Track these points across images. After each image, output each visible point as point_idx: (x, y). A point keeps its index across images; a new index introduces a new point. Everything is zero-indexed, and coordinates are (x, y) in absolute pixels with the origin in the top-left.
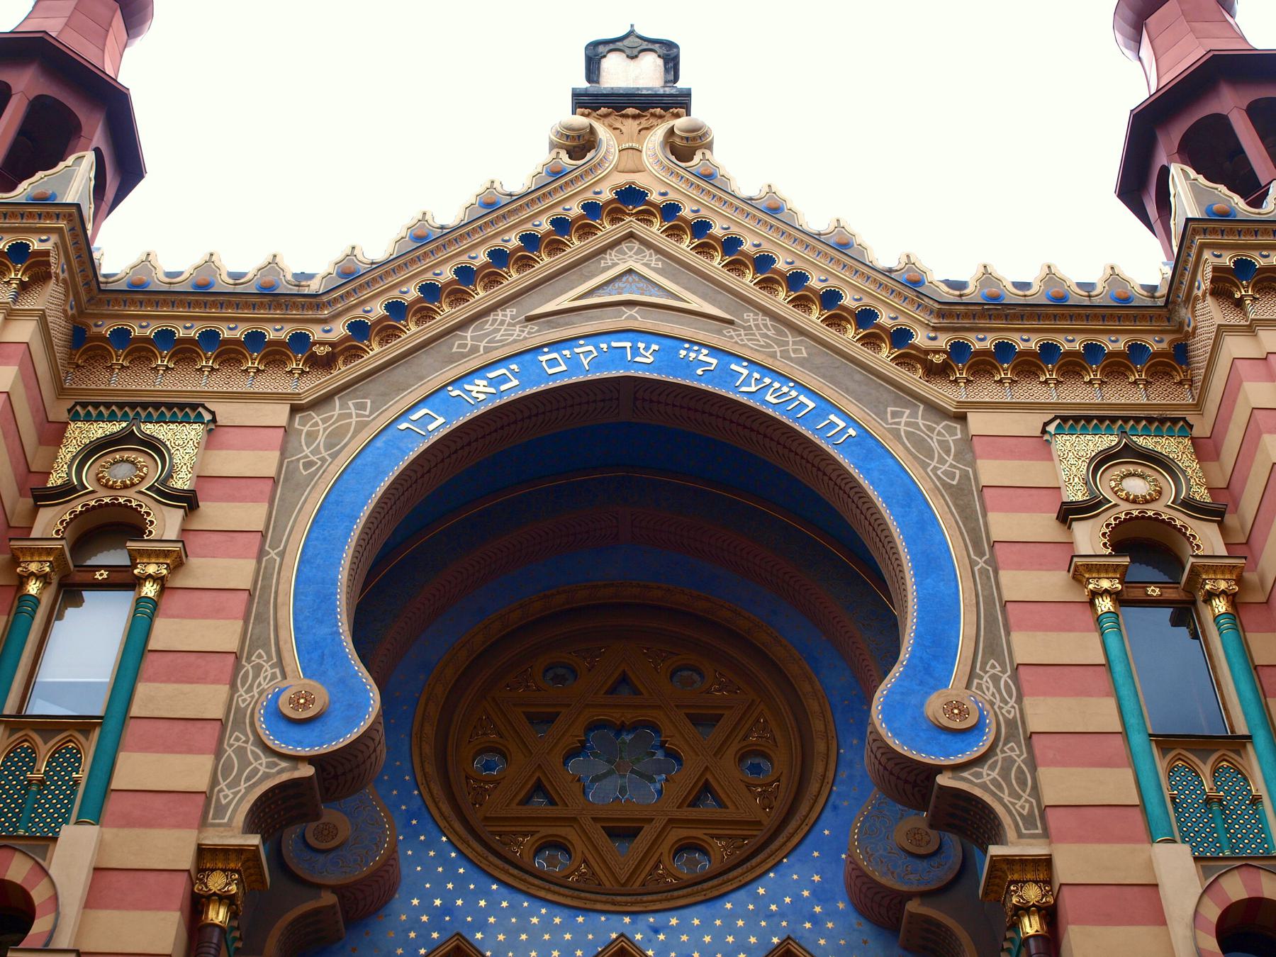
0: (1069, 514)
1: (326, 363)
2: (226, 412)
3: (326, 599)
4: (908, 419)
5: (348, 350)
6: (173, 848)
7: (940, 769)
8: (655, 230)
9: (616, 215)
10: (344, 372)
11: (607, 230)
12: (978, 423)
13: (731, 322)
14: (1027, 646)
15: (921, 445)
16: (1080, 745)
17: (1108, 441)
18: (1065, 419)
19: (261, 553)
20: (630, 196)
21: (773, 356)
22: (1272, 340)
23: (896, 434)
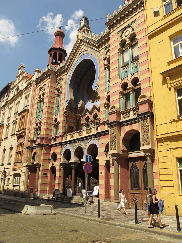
0: (105, 60)
1: (67, 70)
2: (62, 78)
3: (68, 90)
4: (98, 53)
5: (68, 68)
6: (62, 113)
7: (95, 90)
8: (82, 43)
9: (81, 42)
10: (68, 70)
11: (81, 45)
12: (101, 51)
13: (87, 50)
14: (101, 76)
15: (98, 56)
16: (103, 84)
17: (107, 50)
18: (105, 49)
19: (65, 88)
20: (81, 40)
21: (90, 52)
22: (113, 34)
23: (96, 56)
